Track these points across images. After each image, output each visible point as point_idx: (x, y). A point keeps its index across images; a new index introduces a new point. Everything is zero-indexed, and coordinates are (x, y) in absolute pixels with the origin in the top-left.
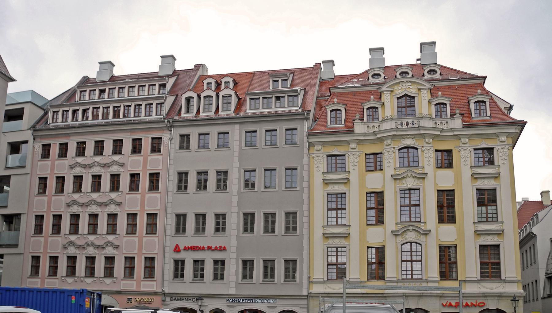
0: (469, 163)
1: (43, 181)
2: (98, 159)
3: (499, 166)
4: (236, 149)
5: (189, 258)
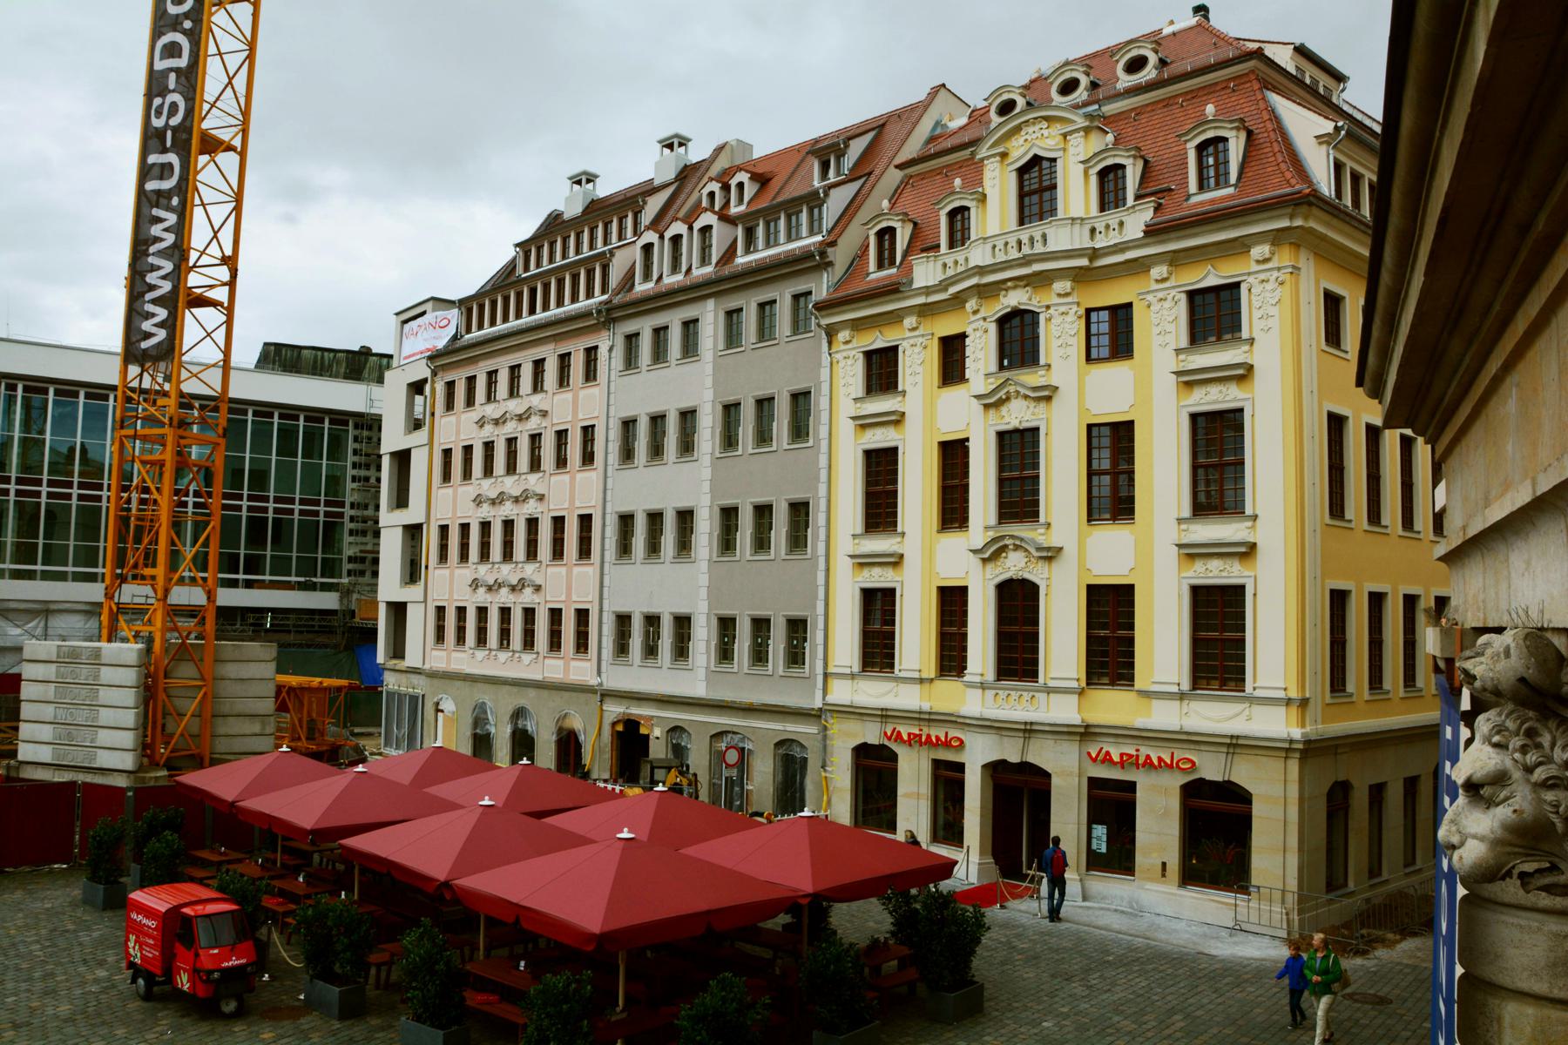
0: (1170, 339)
3: (1251, 341)
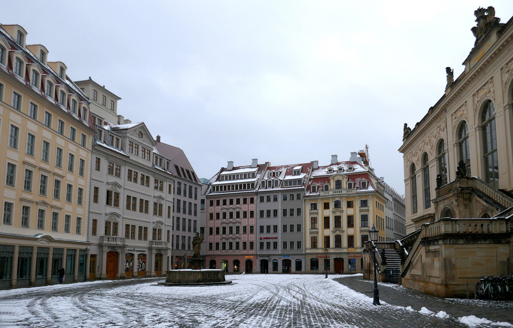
1: (211, 215)
2: (231, 206)
4: (280, 201)
5: (265, 241)
